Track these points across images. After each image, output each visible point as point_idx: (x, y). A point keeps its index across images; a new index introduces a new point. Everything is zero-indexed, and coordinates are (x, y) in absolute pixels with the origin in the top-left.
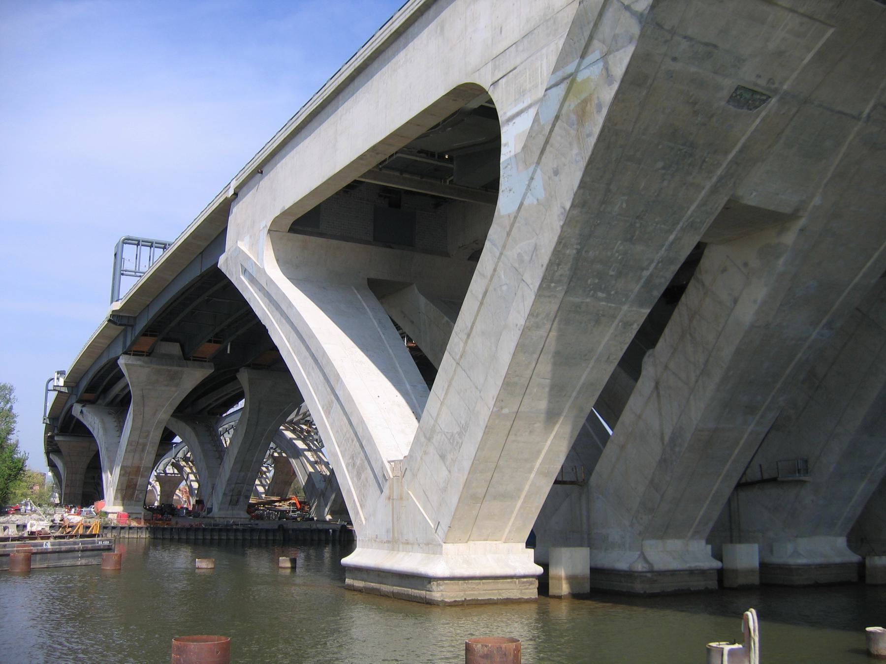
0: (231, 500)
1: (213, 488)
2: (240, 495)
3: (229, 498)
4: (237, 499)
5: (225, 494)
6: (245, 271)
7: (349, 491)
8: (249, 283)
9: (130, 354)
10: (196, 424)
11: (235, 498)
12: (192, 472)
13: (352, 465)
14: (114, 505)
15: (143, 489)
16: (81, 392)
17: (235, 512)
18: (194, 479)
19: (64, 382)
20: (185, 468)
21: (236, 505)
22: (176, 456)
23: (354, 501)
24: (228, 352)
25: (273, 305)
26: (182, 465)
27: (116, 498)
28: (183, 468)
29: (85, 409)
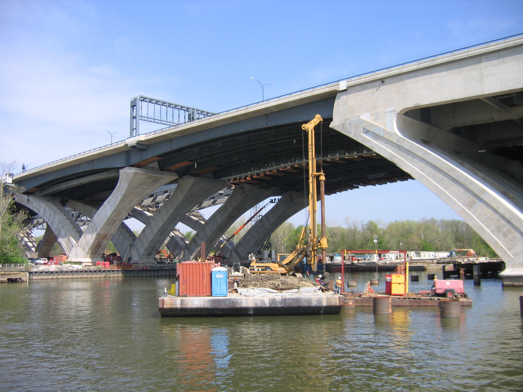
1: (131, 246)
3: (148, 251)
5: (146, 249)
6: (367, 132)
7: (496, 242)
8: (372, 139)
9: (135, 167)
11: (150, 251)
12: (25, 237)
13: (499, 229)
14: (86, 257)
16: (60, 188)
18: (28, 240)
19: (12, 180)
21: (149, 255)
23: (502, 247)
24: (196, 167)
25: (404, 152)
27: (87, 254)
29: (31, 198)
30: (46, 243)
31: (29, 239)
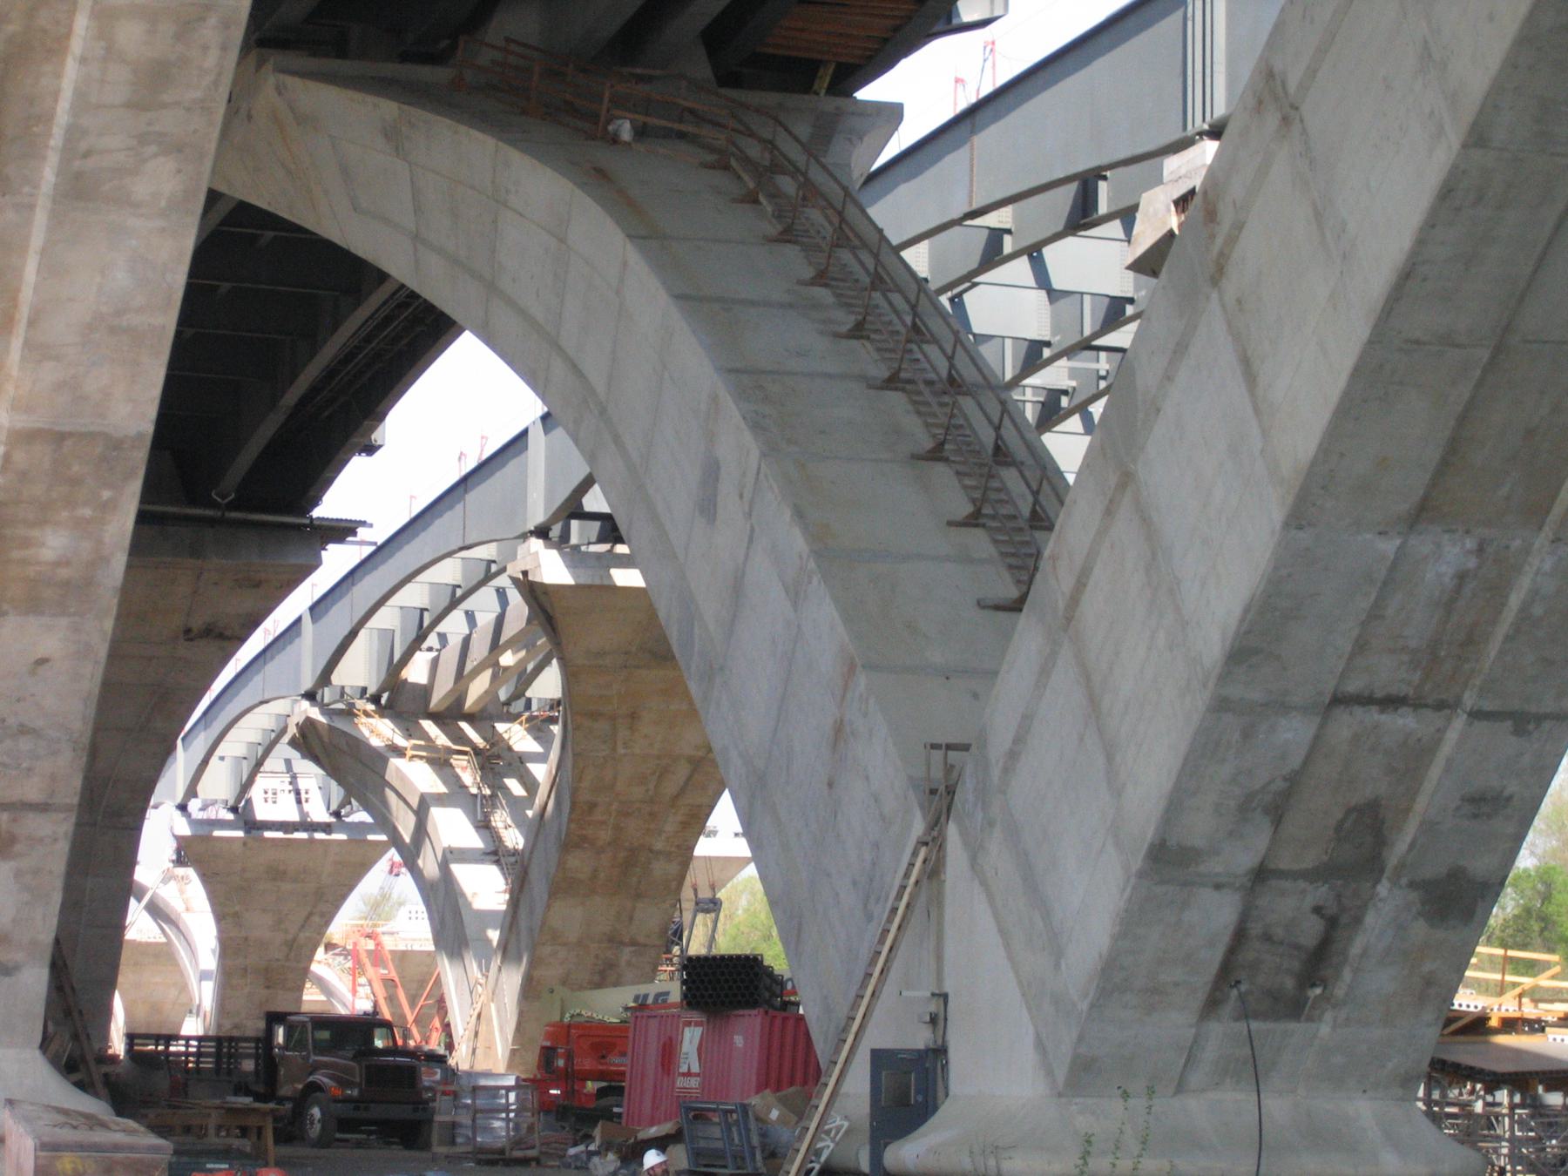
0: (1240, 935)
2: (1371, 865)
4: (1310, 931)
10: (615, 140)
12: (456, 794)
15: (32, 790)
17: (1277, 1107)
18: (474, 840)
20: (395, 762)
21: (1294, 1008)
22: (325, 678)
26: (375, 742)
28: (385, 761)
30: (579, 863)
31: (484, 826)
